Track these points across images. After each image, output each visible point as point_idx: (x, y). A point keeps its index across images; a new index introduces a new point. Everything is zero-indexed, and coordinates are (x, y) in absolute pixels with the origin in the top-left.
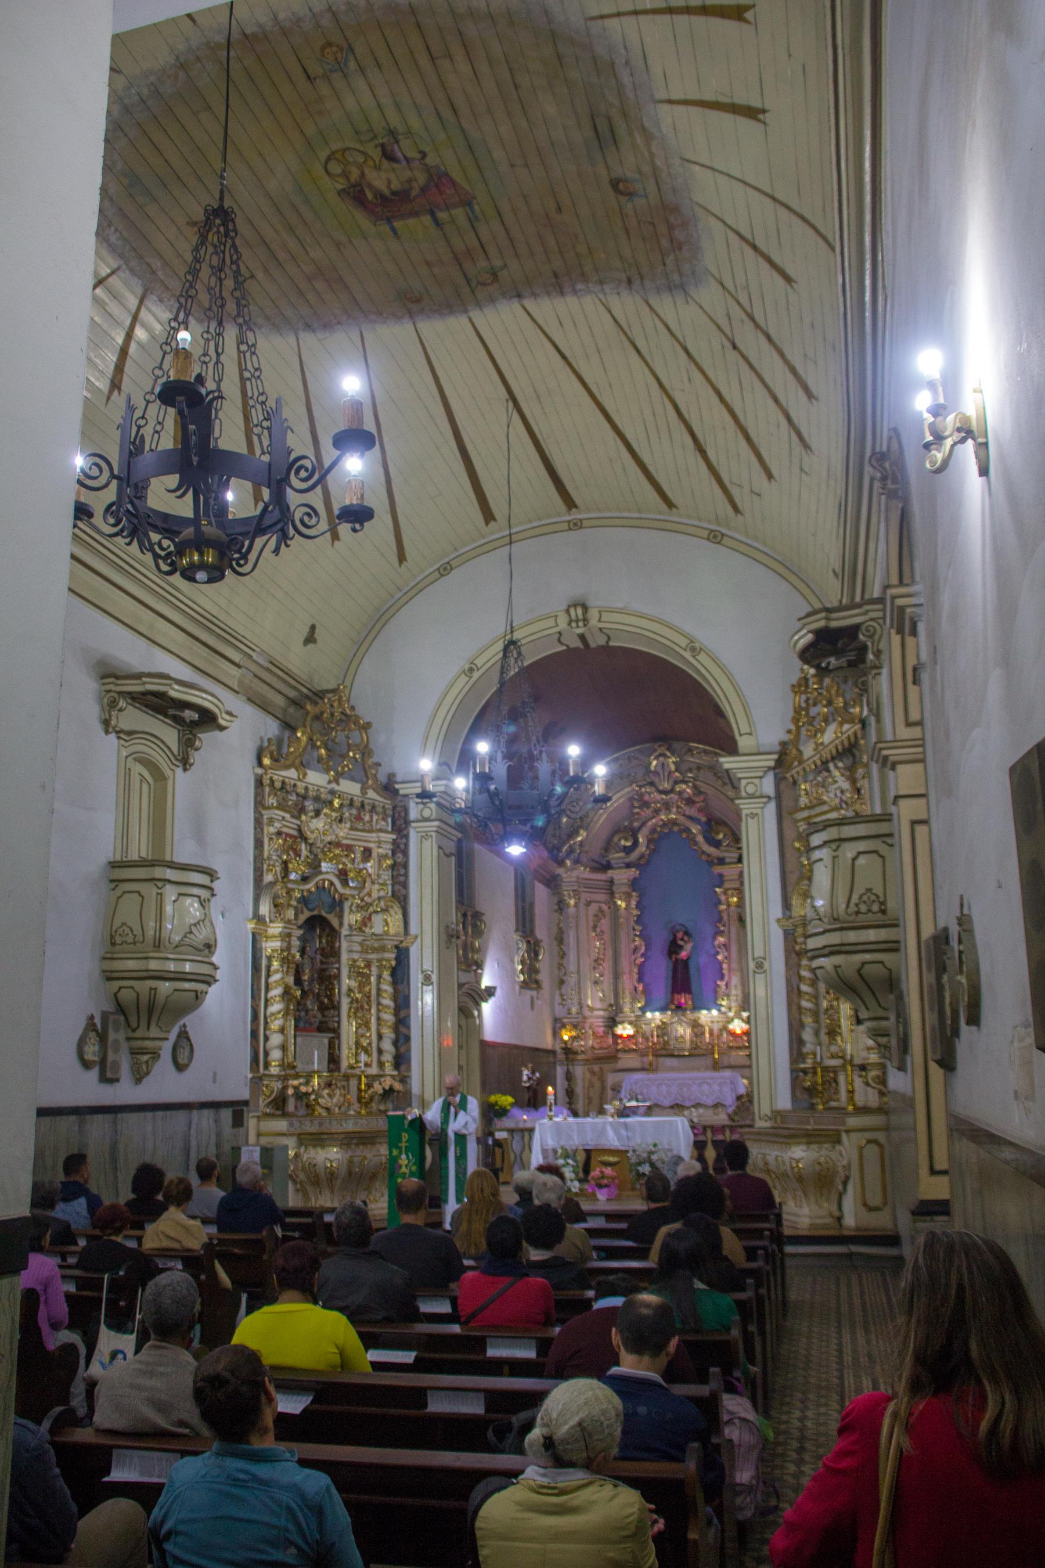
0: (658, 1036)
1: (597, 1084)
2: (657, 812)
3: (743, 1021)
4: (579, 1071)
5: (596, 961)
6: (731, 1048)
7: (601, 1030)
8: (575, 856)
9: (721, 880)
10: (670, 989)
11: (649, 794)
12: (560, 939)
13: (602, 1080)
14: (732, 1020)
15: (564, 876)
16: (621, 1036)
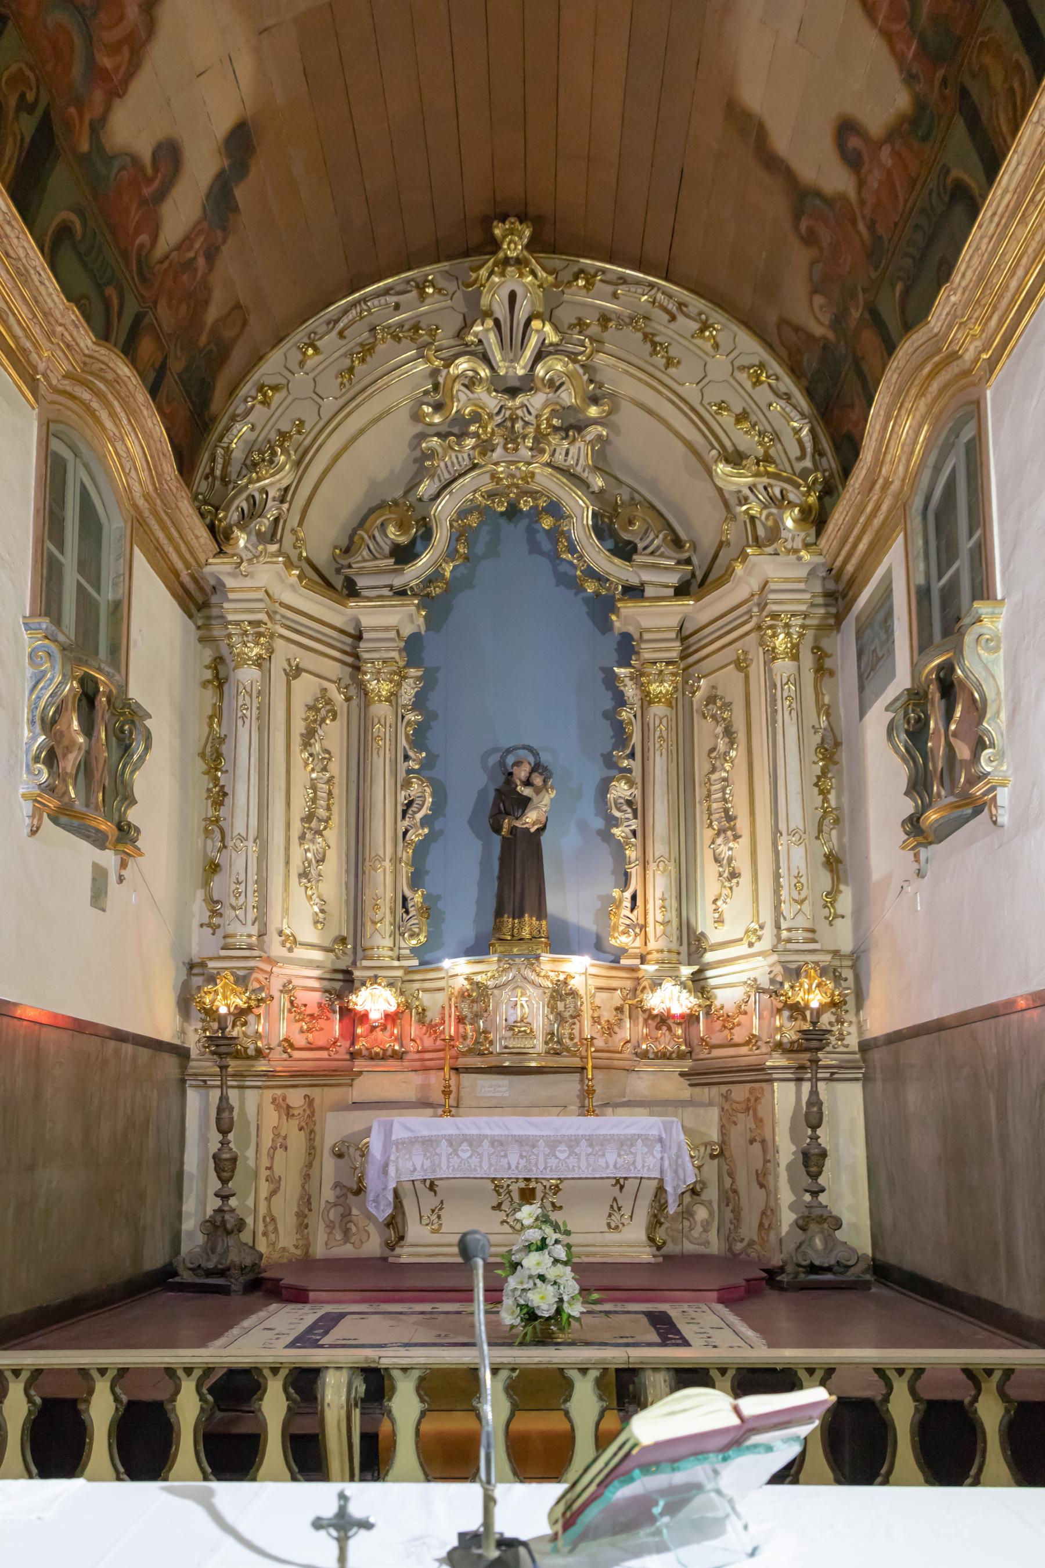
0: (461, 1020)
1: (297, 1141)
2: (485, 447)
3: (684, 985)
4: (253, 1104)
5: (309, 818)
6: (645, 1055)
7: (313, 999)
8: (263, 525)
9: (627, 648)
10: (492, 904)
11: (471, 383)
12: (214, 756)
13: (310, 1129)
14: (656, 984)
15: (230, 583)
16: (364, 1017)
